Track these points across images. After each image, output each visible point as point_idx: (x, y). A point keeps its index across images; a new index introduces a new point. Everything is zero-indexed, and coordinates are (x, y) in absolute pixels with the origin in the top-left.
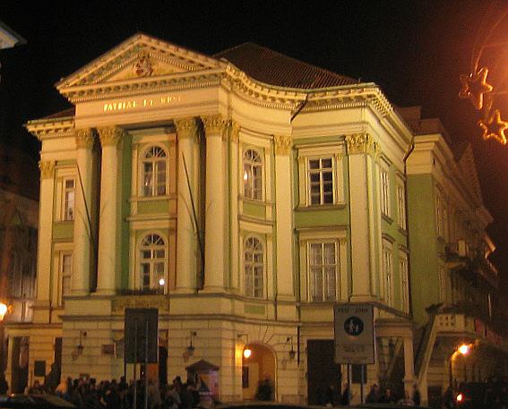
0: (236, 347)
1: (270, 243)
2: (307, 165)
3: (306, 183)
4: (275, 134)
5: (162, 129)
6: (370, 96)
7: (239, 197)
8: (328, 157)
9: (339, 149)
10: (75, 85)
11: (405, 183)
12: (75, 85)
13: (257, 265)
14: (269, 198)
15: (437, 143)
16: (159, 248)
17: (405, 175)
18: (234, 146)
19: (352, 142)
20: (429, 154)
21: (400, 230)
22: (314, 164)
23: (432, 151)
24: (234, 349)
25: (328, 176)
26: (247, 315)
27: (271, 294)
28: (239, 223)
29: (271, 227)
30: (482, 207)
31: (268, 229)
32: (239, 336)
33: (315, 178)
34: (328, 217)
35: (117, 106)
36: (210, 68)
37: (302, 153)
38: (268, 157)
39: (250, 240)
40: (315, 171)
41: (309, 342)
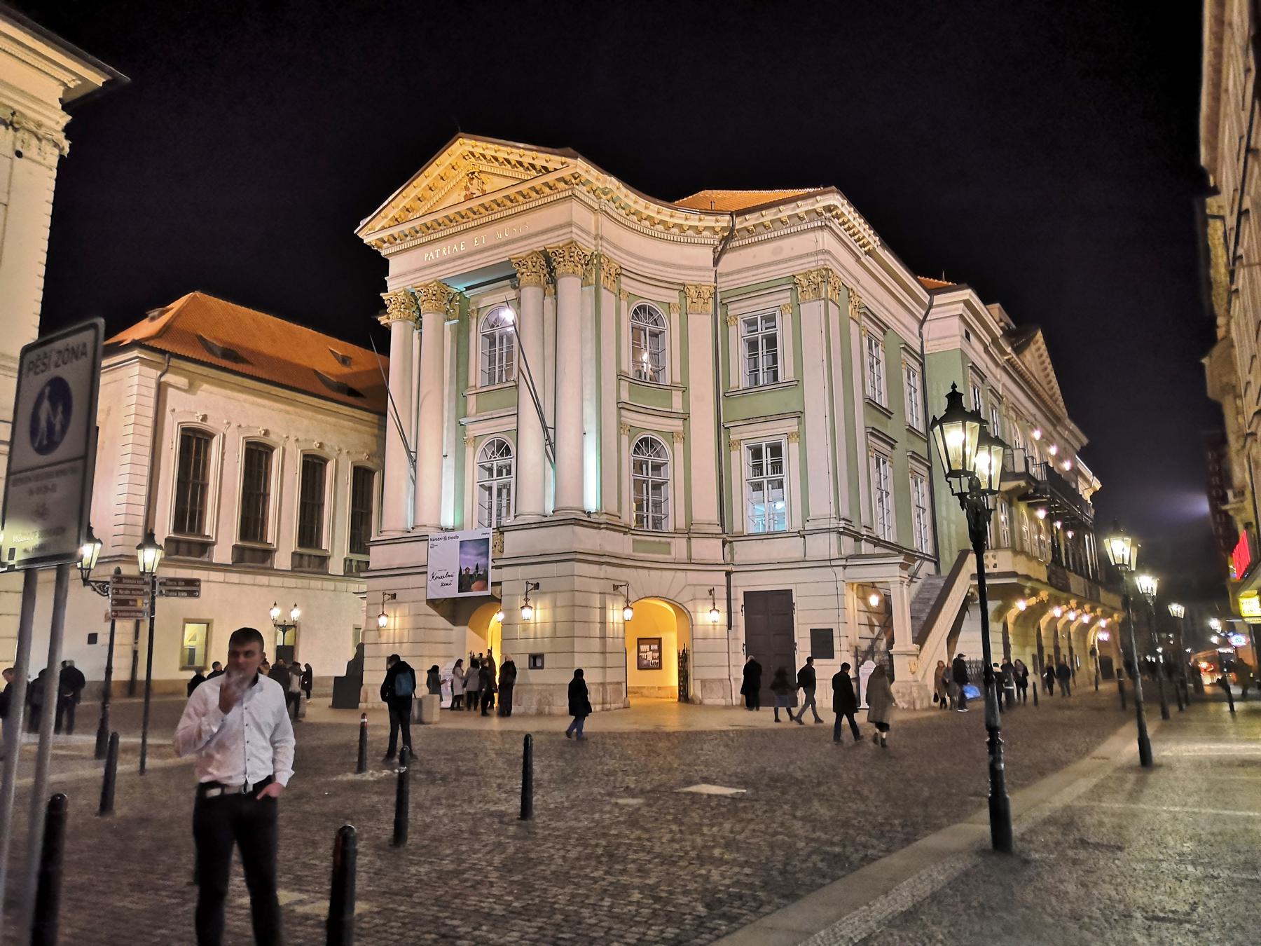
0: (609, 605)
1: (679, 446)
2: (743, 329)
3: (738, 353)
4: (686, 282)
5: (507, 282)
6: (829, 209)
7: (621, 376)
8: (770, 312)
9: (785, 298)
10: (383, 228)
11: (922, 365)
12: (383, 228)
13: (657, 479)
14: (677, 378)
15: (967, 303)
16: (504, 461)
17: (922, 356)
18: (608, 299)
19: (805, 283)
20: (957, 320)
21: (911, 430)
22: (751, 323)
23: (961, 316)
24: (603, 609)
25: (771, 341)
26: (637, 554)
27: (681, 523)
28: (619, 416)
29: (680, 422)
30: (1068, 421)
31: (677, 425)
32: (616, 588)
33: (753, 345)
34: (769, 402)
35: (440, 252)
36: (556, 170)
37: (733, 309)
38: (675, 317)
39: (644, 441)
40: (752, 336)
41: (747, 595)
